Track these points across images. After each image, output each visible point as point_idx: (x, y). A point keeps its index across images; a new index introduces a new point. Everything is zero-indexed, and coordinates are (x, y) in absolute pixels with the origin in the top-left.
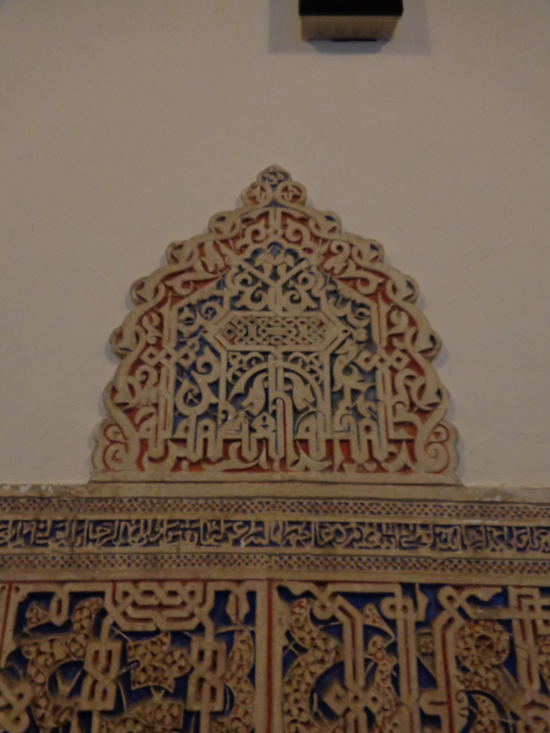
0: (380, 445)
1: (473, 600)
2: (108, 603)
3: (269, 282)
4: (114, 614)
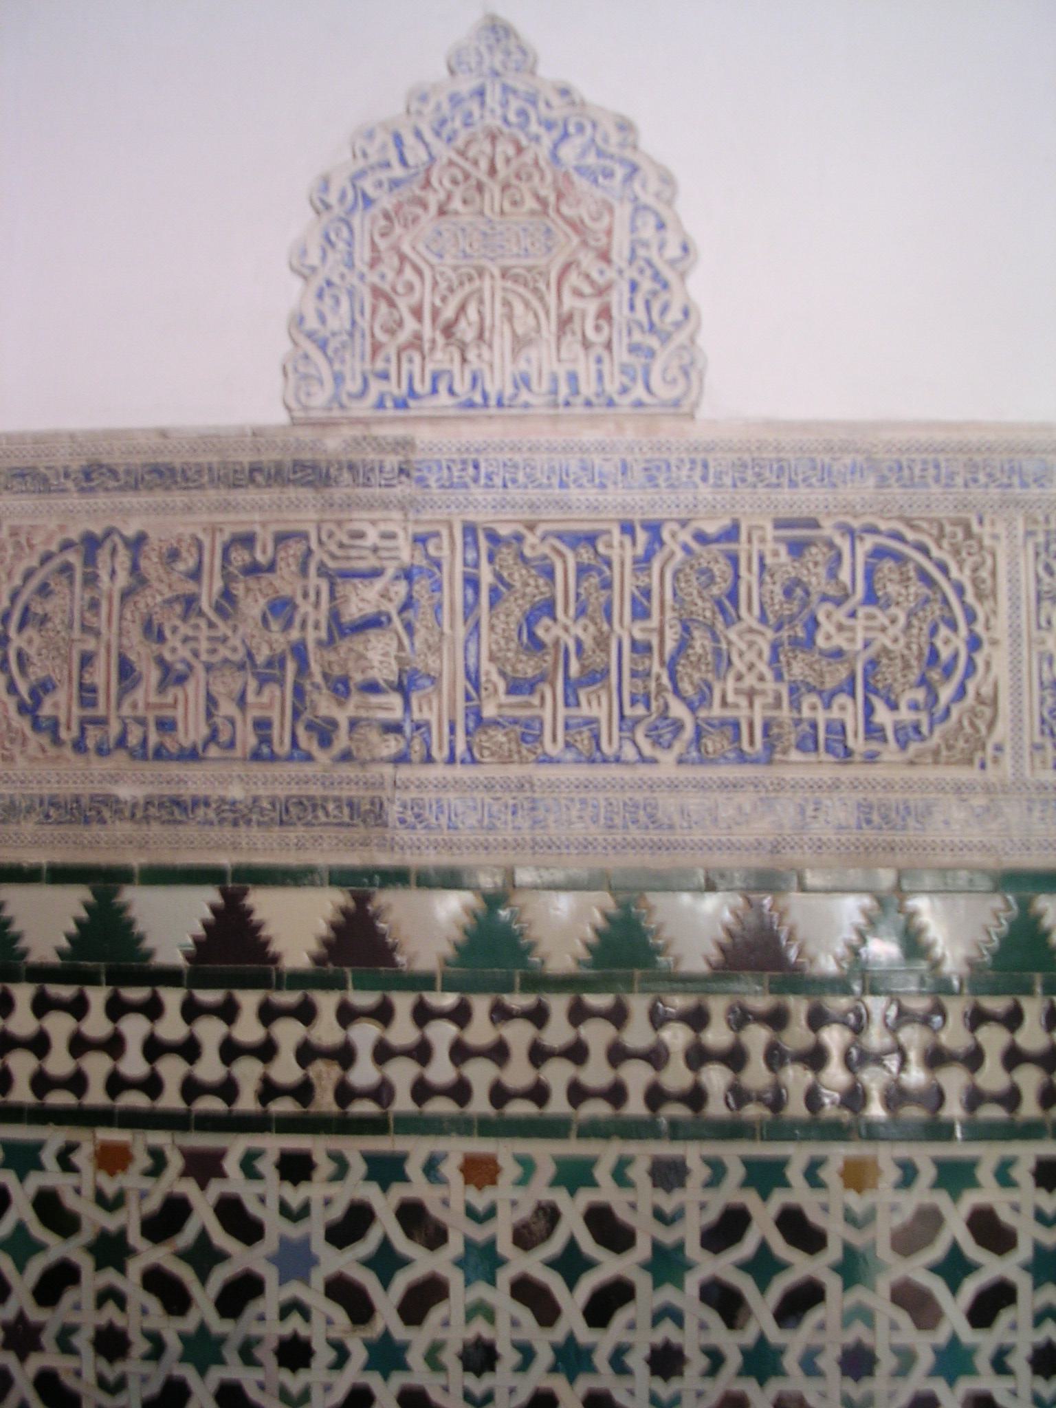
0: (612, 374)
1: (701, 537)
2: (314, 545)
3: (485, 179)
4: (319, 555)
